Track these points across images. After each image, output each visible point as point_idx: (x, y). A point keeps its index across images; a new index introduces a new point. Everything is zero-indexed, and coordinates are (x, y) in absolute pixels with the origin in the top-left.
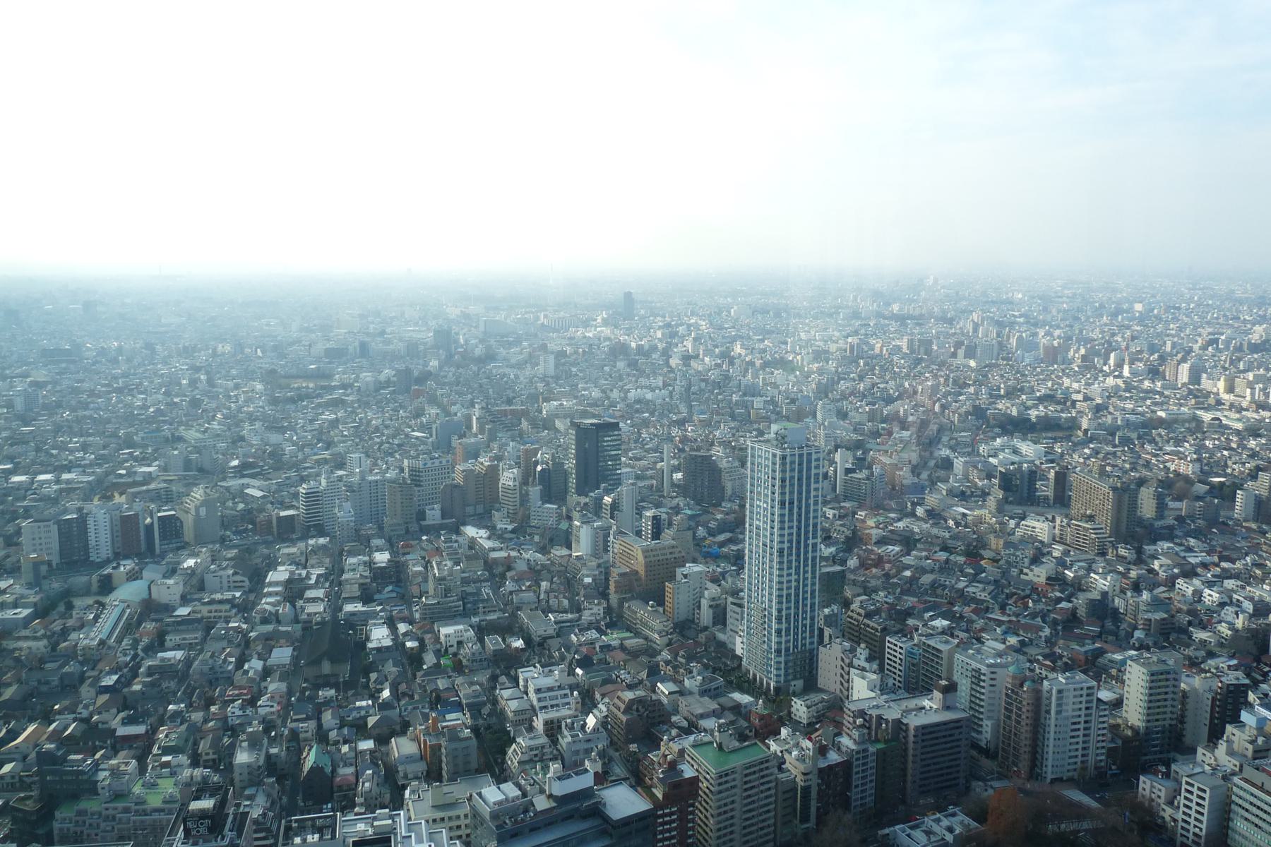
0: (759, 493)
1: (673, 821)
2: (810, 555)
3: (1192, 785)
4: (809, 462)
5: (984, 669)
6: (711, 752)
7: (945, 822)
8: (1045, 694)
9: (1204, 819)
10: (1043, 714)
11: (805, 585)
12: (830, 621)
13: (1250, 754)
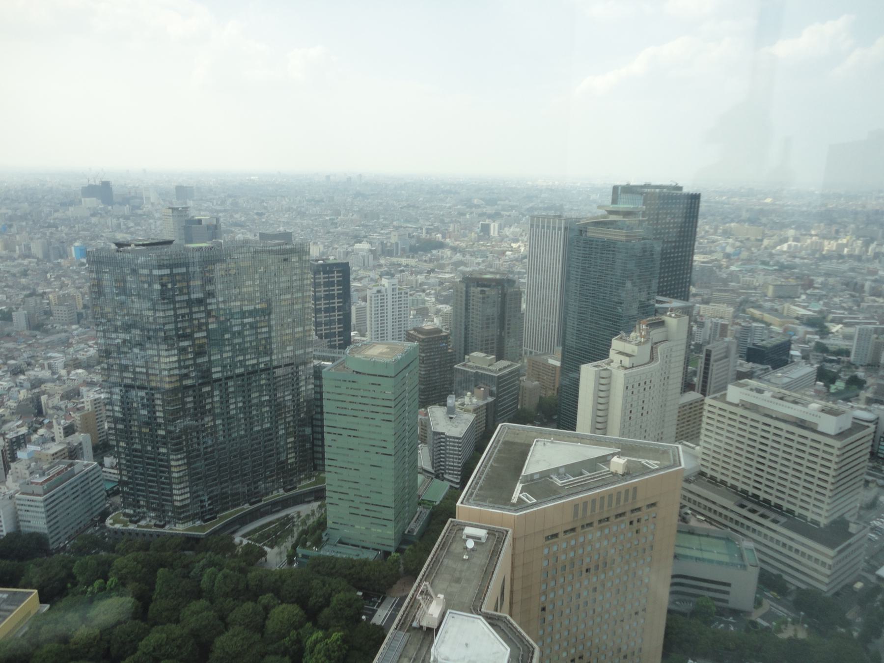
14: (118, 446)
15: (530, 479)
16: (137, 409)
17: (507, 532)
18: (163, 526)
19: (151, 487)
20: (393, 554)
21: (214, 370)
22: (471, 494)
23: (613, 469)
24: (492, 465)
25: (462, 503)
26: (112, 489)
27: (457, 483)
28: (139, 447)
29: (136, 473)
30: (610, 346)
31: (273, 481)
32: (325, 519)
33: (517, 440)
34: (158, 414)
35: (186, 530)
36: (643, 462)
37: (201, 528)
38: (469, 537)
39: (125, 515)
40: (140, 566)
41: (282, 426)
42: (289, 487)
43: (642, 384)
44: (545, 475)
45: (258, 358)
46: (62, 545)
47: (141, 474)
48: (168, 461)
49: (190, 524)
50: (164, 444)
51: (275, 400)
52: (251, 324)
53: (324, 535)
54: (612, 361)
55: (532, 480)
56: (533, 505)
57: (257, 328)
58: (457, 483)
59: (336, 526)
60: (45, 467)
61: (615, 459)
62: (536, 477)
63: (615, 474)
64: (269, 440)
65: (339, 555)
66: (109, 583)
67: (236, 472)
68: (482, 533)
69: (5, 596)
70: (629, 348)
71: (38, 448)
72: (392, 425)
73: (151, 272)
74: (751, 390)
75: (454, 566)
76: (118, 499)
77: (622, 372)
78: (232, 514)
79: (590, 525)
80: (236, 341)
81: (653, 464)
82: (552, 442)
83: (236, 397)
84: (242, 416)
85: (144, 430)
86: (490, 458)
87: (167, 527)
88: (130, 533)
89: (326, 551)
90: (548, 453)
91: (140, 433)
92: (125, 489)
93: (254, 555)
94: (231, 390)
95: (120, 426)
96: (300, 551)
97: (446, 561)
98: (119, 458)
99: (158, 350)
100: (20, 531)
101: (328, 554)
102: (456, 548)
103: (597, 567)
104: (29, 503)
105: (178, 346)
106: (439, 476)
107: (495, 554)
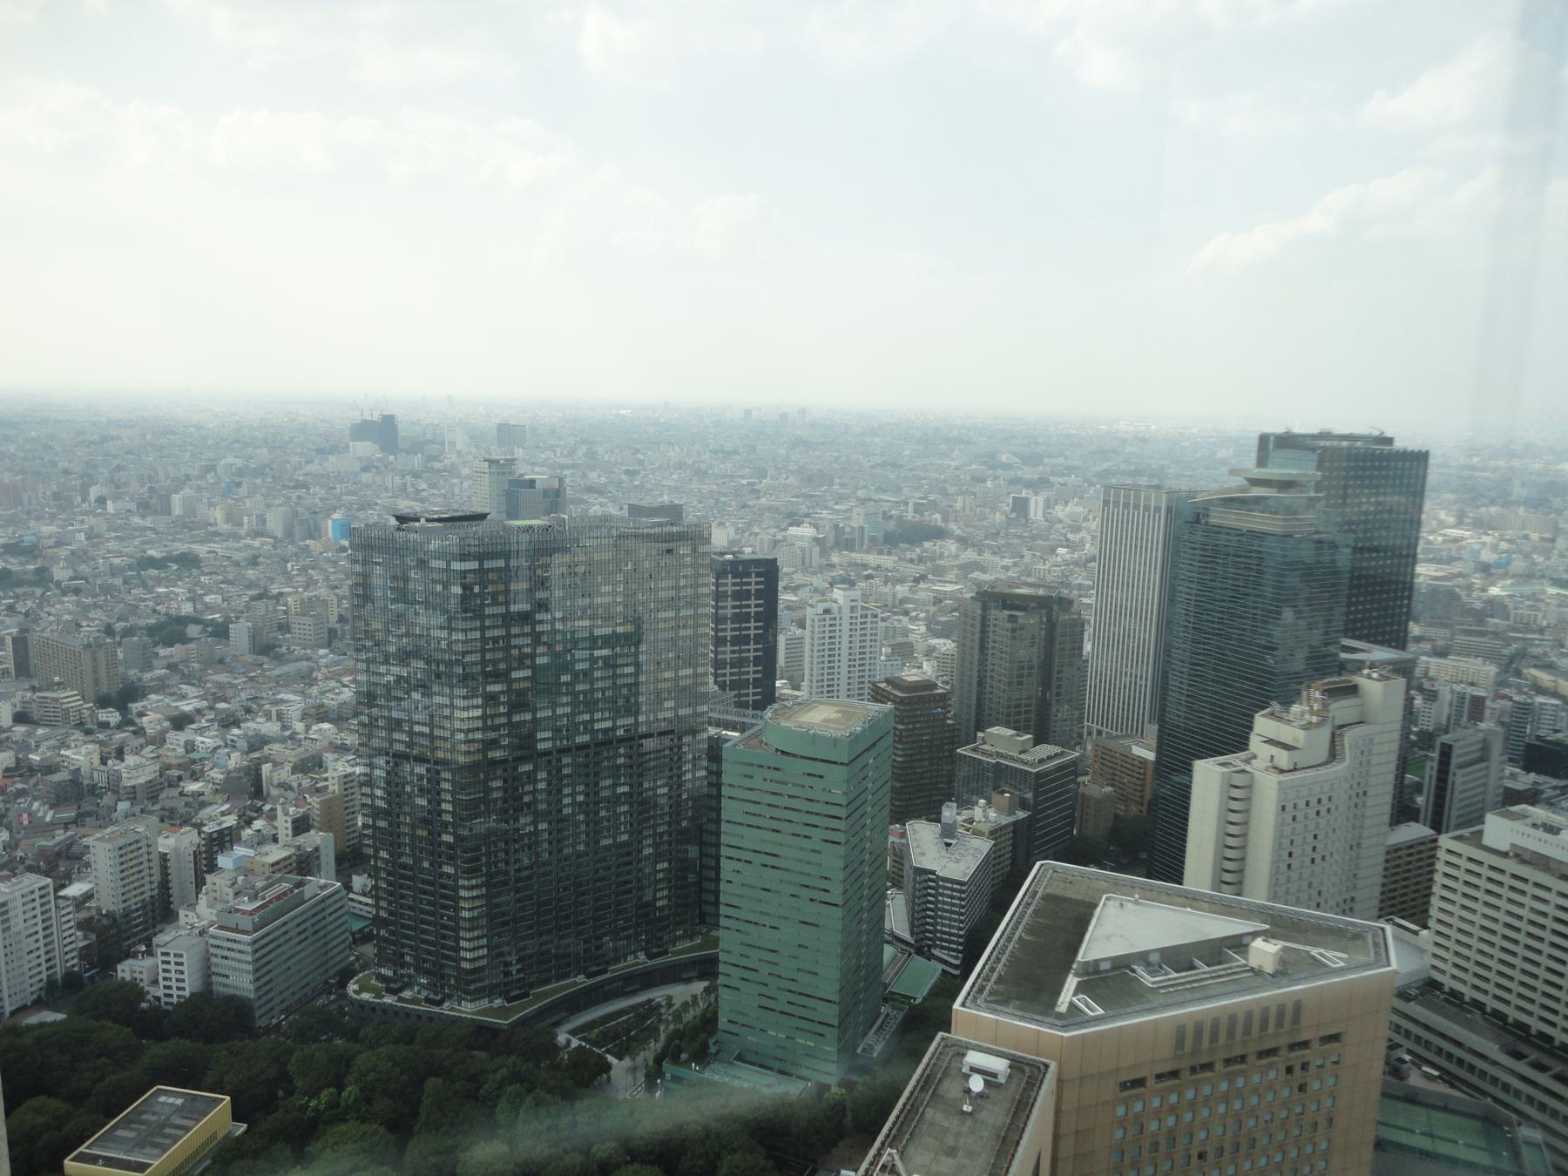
3: (167, 954)
13: (231, 897)
14: (376, 857)
15: (1092, 969)
16: (410, 796)
17: (1047, 1066)
18: (439, 1003)
19: (424, 932)
20: (834, 1090)
22: (981, 990)
23: (1254, 962)
24: (1020, 938)
25: (963, 1005)
26: (361, 931)
27: (956, 967)
28: (410, 861)
30: (1251, 728)
31: (628, 938)
32: (715, 1013)
33: (1069, 894)
34: (444, 806)
36: (1314, 952)
38: (974, 1070)
39: (380, 977)
40: (398, 1070)
41: (650, 841)
42: (655, 950)
43: (1313, 802)
44: (1122, 964)
45: (614, 719)
46: (274, 1021)
47: (411, 908)
48: (456, 888)
49: (484, 1004)
50: (452, 858)
51: (640, 794)
52: (605, 659)
53: (711, 1042)
54: (1255, 757)
55: (1097, 972)
56: (1098, 1020)
57: (615, 666)
58: (956, 967)
59: (731, 1028)
60: (259, 885)
61: (1258, 943)
62: (1105, 966)
63: (1257, 972)
64: (625, 864)
67: (567, 917)
68: (999, 1065)
69: (179, 1102)
70: (1287, 733)
71: (251, 853)
72: (841, 850)
73: (449, 564)
74: (1534, 825)
75: (946, 1124)
76: (369, 950)
77: (1275, 778)
78: (555, 991)
79: (1208, 1066)
81: (1334, 957)
82: (1136, 903)
84: (582, 817)
85: (420, 832)
86: (1018, 923)
87: (446, 1004)
88: (385, 1009)
90: (1128, 922)
91: (413, 836)
92: (382, 932)
94: (566, 771)
95: (382, 824)
97: (930, 1112)
99: (452, 697)
100: (211, 991)
102: (951, 1089)
103: (1220, 1151)
104: (230, 945)
106: (922, 948)
107: (1022, 1108)
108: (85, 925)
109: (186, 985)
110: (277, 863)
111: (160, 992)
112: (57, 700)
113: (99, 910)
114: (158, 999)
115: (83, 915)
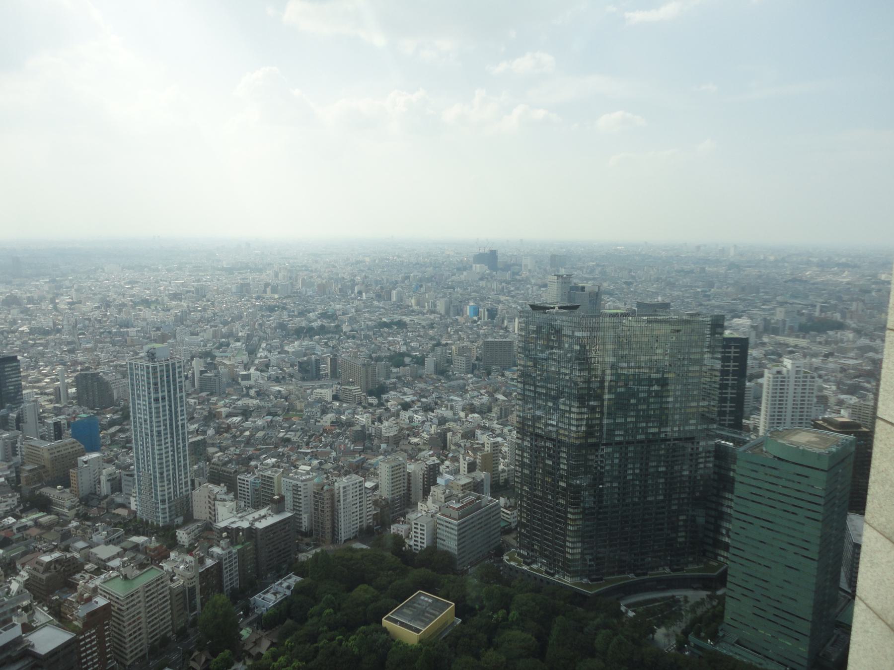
0: (139, 396)
1: (93, 640)
2: (180, 432)
4: (174, 369)
5: (299, 483)
6: (119, 582)
7: (285, 585)
8: (336, 492)
9: (425, 541)
10: (336, 503)
11: (178, 453)
12: (199, 473)
13: (443, 500)
14: (522, 489)
18: (553, 575)
19: (546, 534)
21: (617, 433)
28: (540, 494)
29: (534, 518)
32: (722, 612)
34: (562, 466)
35: (575, 584)
37: (586, 586)
39: (520, 555)
41: (676, 502)
42: (675, 567)
45: (660, 428)
47: (539, 520)
48: (566, 513)
49: (577, 580)
50: (563, 495)
51: (672, 473)
53: (720, 628)
57: (662, 397)
59: (732, 623)
60: (460, 495)
65: (738, 657)
66: (511, 615)
69: (430, 601)
71: (452, 478)
73: (573, 332)
76: (510, 539)
80: (641, 407)
83: (634, 464)
85: (547, 479)
87: (557, 576)
89: (724, 649)
91: (543, 481)
93: (642, 630)
94: (630, 455)
95: (526, 472)
96: (692, 638)
98: (522, 501)
99: (570, 406)
100: (436, 547)
101: (725, 651)
105: (588, 405)
108: (375, 503)
109: (425, 541)
110: (465, 485)
111: (412, 543)
112: (350, 390)
113: (381, 496)
114: (410, 546)
115: (374, 498)
